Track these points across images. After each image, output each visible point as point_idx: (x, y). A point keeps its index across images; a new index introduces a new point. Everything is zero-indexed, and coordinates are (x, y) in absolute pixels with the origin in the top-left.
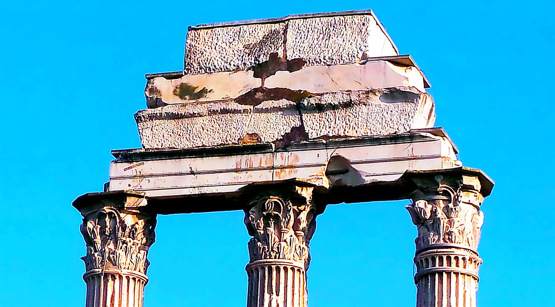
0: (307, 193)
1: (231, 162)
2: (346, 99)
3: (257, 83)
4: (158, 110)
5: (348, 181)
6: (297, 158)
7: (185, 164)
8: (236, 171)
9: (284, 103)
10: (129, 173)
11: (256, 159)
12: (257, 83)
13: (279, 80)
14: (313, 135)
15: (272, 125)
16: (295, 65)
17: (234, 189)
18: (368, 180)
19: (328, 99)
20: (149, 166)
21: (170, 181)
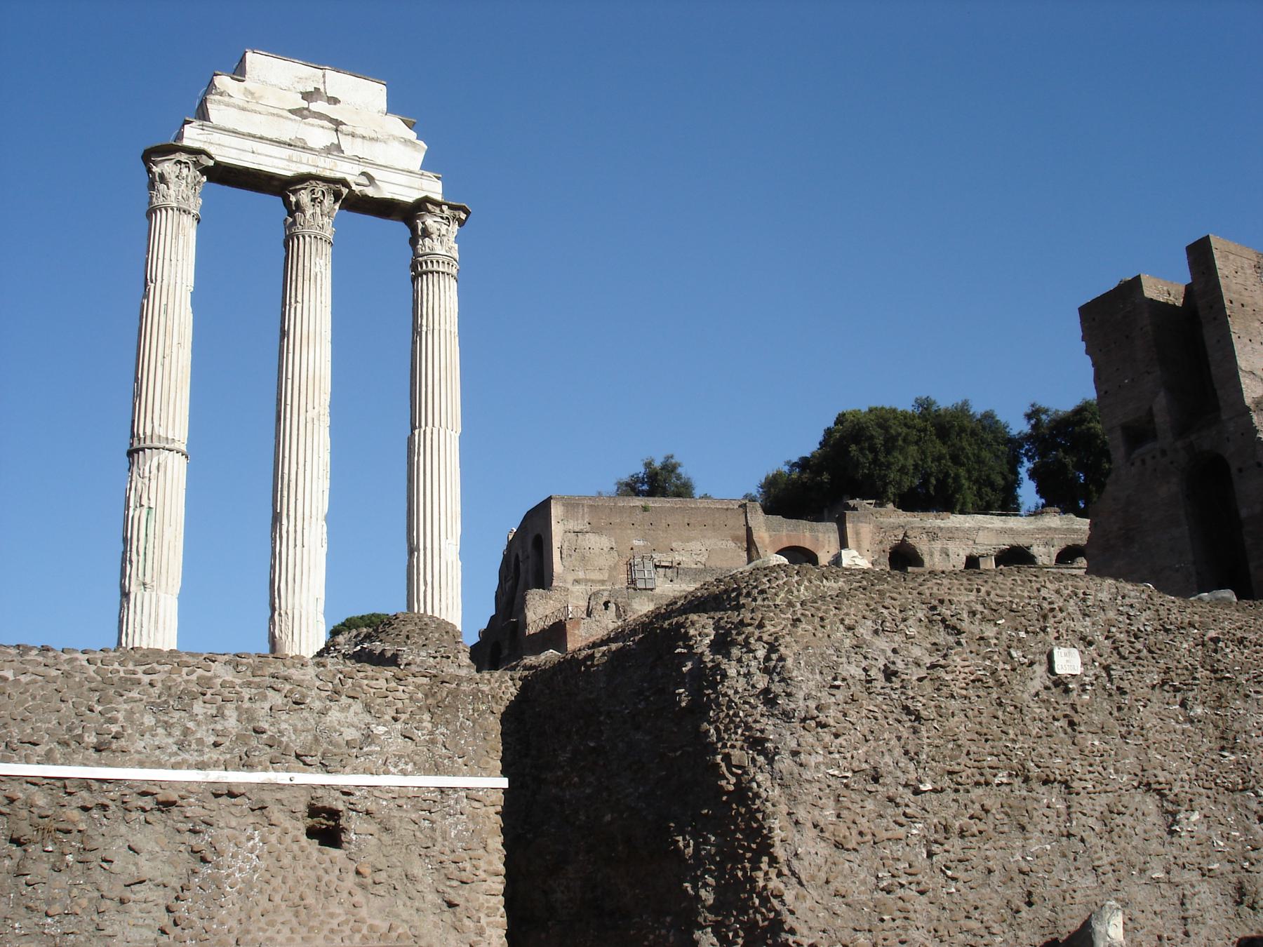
0: (345, 191)
1: (286, 152)
2: (373, 135)
3: (305, 104)
4: (226, 99)
5: (371, 192)
6: (336, 165)
7: (249, 144)
8: (290, 160)
9: (326, 124)
10: (200, 137)
11: (305, 156)
12: (305, 104)
13: (319, 106)
14: (347, 153)
15: (319, 136)
16: (334, 101)
17: (289, 174)
18: (389, 196)
19: (359, 131)
20: (217, 137)
21: (234, 153)
